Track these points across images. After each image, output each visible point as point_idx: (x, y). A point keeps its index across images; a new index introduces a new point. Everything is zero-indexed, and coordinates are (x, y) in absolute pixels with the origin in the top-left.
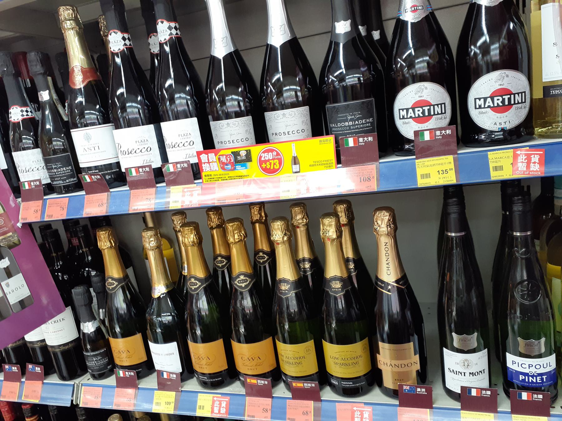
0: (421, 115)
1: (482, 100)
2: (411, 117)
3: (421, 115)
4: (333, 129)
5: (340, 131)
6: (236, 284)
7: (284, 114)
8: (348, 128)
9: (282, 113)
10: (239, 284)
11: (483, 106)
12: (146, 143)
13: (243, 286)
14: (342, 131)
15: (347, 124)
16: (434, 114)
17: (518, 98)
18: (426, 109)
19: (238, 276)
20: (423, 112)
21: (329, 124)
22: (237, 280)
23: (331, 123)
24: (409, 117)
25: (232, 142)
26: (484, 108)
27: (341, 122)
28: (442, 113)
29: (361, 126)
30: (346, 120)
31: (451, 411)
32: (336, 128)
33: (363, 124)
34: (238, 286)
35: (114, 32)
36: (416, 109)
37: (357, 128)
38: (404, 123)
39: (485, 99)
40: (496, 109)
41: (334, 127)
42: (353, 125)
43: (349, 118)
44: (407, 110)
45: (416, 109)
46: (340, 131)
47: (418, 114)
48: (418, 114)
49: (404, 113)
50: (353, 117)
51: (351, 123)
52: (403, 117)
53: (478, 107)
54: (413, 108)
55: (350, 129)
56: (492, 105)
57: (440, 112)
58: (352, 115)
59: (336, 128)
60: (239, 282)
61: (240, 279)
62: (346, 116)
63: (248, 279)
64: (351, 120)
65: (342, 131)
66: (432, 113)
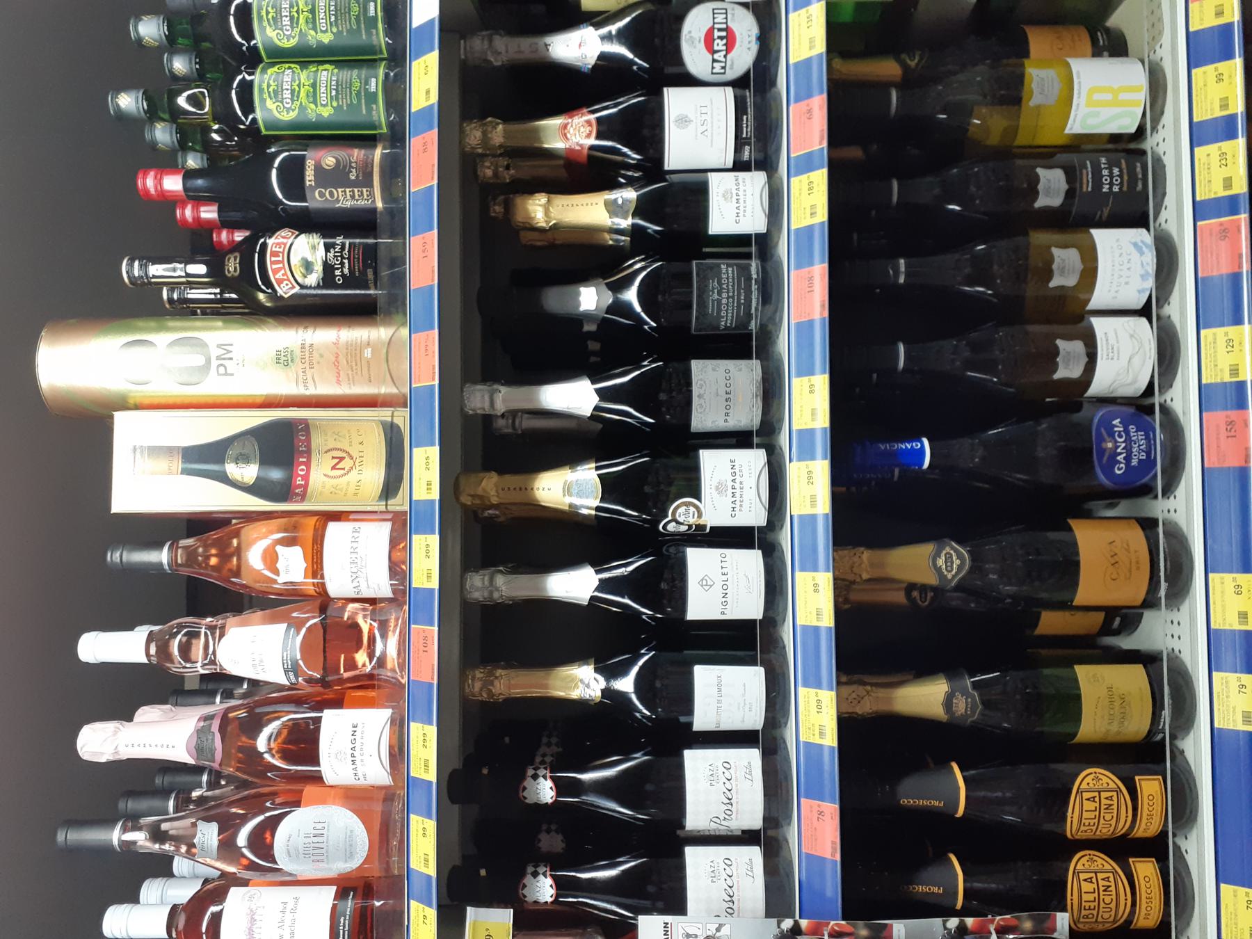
0: (725, 41)
1: (715, 64)
2: (725, 56)
3: (725, 41)
4: (728, 325)
5: (733, 313)
6: (954, 577)
7: (700, 396)
8: (731, 300)
9: (697, 399)
10: (954, 571)
11: (723, 65)
12: (715, 769)
13: (958, 562)
14: (733, 309)
15: (724, 301)
16: (726, 23)
17: (720, 18)
18: (717, 34)
19: (938, 570)
20: (721, 38)
21: (719, 330)
22: (946, 573)
23: (718, 328)
24: (724, 60)
25: (729, 396)
26: (726, 62)
27: (719, 310)
28: (726, 13)
29: (730, 280)
30: (719, 302)
31: (1204, 426)
32: (726, 321)
33: (728, 278)
34: (957, 573)
35: (523, 792)
36: (716, 48)
37: (733, 286)
38: (732, 68)
39: (714, 61)
40: (730, 46)
41: (726, 323)
42: (728, 292)
43: (716, 296)
44: (714, 61)
45: (716, 48)
46: (733, 313)
47: (723, 45)
48: (723, 45)
49: (717, 66)
50: (716, 291)
51: (724, 295)
52: (724, 68)
53: (723, 71)
54: (713, 52)
55: (733, 297)
56: (724, 53)
57: (724, 16)
58: (713, 293)
59: (726, 321)
60: (949, 568)
61: (944, 566)
62: (713, 301)
63: (944, 552)
64: (720, 293)
65: (733, 309)
66: (724, 26)
